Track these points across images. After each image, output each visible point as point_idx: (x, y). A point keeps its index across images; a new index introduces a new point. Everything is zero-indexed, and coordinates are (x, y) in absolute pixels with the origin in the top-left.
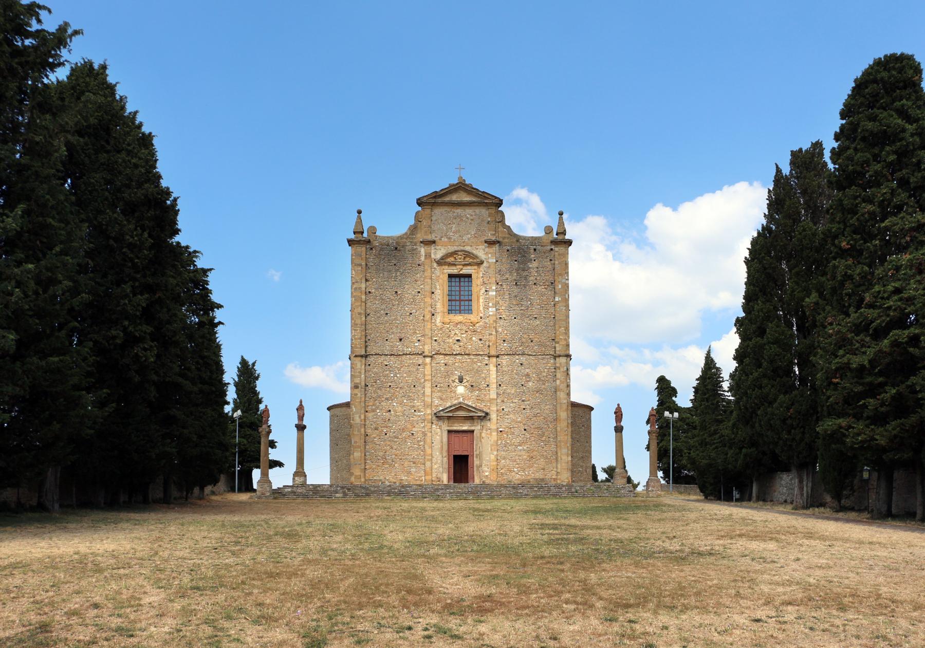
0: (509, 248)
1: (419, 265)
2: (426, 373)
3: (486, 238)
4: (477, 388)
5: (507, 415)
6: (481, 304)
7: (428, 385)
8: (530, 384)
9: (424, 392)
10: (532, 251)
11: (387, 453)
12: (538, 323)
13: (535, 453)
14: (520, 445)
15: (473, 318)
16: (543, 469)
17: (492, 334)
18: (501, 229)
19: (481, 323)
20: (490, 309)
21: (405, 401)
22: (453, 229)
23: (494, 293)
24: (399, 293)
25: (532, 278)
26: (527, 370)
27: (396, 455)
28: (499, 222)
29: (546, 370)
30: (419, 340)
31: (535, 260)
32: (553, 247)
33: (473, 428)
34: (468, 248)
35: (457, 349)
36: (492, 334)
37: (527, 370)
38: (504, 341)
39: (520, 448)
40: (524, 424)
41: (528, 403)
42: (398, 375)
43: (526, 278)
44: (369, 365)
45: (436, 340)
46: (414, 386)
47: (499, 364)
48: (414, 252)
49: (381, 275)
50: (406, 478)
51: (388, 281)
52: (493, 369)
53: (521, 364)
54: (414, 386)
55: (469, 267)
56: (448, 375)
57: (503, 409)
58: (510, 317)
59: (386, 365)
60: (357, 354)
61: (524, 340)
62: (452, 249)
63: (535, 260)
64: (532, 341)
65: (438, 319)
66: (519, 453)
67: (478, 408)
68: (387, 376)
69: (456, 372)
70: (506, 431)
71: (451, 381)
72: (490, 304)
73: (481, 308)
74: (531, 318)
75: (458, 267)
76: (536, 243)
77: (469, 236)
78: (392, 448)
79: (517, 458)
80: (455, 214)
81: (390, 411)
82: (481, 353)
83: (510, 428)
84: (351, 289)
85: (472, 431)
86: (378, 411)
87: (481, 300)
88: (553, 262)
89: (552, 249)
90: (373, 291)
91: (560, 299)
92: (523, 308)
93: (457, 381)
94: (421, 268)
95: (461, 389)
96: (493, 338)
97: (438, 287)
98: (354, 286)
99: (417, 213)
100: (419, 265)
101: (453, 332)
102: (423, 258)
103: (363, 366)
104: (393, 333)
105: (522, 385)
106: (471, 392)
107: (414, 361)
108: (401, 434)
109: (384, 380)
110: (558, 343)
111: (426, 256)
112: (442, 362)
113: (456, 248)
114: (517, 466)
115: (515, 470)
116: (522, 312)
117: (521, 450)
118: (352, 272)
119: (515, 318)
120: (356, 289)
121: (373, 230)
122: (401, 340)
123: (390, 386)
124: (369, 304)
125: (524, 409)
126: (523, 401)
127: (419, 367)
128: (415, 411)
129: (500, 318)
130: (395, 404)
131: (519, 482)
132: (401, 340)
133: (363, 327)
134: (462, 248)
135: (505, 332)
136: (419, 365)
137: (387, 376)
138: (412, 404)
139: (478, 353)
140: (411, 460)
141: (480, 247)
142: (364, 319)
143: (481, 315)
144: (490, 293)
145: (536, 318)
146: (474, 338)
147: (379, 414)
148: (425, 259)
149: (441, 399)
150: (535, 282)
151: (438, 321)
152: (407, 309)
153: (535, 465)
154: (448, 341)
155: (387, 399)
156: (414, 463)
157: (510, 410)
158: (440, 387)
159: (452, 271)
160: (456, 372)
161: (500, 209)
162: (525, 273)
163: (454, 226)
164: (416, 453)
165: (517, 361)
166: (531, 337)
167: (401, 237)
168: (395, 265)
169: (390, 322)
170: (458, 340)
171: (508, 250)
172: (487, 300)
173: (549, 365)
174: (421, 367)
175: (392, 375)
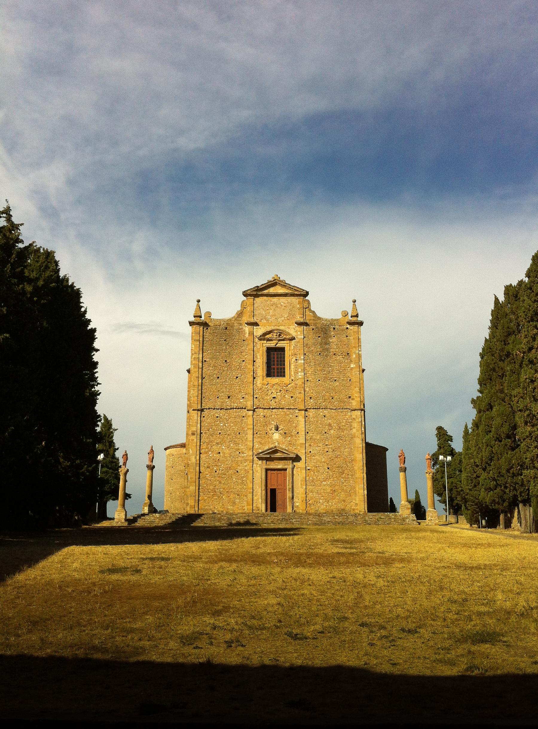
0: (314, 327)
1: (244, 340)
2: (249, 423)
3: (296, 320)
4: (289, 435)
5: (314, 456)
6: (292, 369)
7: (250, 432)
8: (332, 432)
9: (247, 438)
10: (332, 329)
11: (217, 487)
12: (338, 384)
13: (337, 488)
14: (324, 481)
15: (285, 380)
16: (344, 501)
17: (301, 393)
18: (308, 313)
19: (292, 384)
20: (300, 374)
21: (232, 445)
22: (271, 313)
23: (303, 361)
24: (228, 361)
25: (331, 350)
26: (330, 421)
27: (224, 489)
28: (306, 308)
29: (344, 421)
30: (243, 398)
31: (334, 336)
32: (348, 326)
33: (286, 467)
34: (282, 328)
35: (273, 404)
36: (301, 393)
37: (330, 421)
38: (311, 398)
39: (325, 483)
40: (328, 464)
41: (331, 446)
42: (226, 425)
43: (327, 350)
44: (204, 417)
45: (256, 398)
46: (239, 433)
47: (307, 416)
48: (240, 331)
49: (215, 348)
50: (231, 507)
51: (219, 352)
52: (301, 419)
53: (325, 416)
54: (239, 433)
55: (282, 342)
56: (266, 424)
57: (310, 452)
58: (315, 380)
59: (217, 417)
60: (194, 408)
61: (326, 397)
62: (269, 329)
63: (334, 336)
64: (333, 398)
65: (259, 382)
66: (324, 488)
67: (290, 450)
68: (218, 425)
69: (273, 422)
70: (313, 469)
71: (268, 430)
72: (300, 370)
73: (293, 373)
74: (331, 380)
75: (274, 342)
76: (335, 324)
77: (283, 319)
78: (220, 483)
79: (322, 491)
80: (272, 302)
81: (219, 453)
82: (292, 407)
83: (316, 467)
84: (191, 358)
85: (286, 470)
86: (210, 453)
87: (292, 367)
88: (348, 338)
89: (347, 328)
90: (208, 360)
91: (355, 366)
92: (325, 373)
93: (273, 429)
94: (246, 343)
95: (276, 436)
96: (302, 396)
97: (259, 357)
98: (194, 356)
99: (243, 302)
100: (244, 340)
101: (270, 392)
102: (247, 335)
103: (199, 418)
104: (223, 392)
105: (325, 433)
106: (285, 438)
107: (239, 414)
108: (228, 472)
109: (215, 429)
110: (353, 399)
111: (249, 333)
112: (261, 414)
113: (273, 328)
114: (322, 498)
115: (321, 501)
116: (324, 375)
117: (325, 485)
118: (192, 346)
119: (319, 380)
120: (195, 358)
121: (209, 314)
122: (229, 397)
123: (220, 433)
124: (204, 370)
125: (327, 451)
126: (326, 445)
127: (243, 418)
128: (240, 453)
129: (308, 380)
130: (223, 447)
131: (324, 512)
132: (229, 397)
133: (200, 388)
134: (278, 328)
135: (312, 391)
136: (243, 417)
137: (218, 425)
138: (237, 447)
139: (290, 407)
140: (236, 493)
141: (292, 327)
142: (200, 381)
143: (292, 378)
144: (299, 362)
145: (335, 380)
146: (286, 396)
147: (210, 455)
148: (249, 336)
149: (261, 443)
150: (335, 353)
151: (258, 382)
152: (234, 373)
153: (337, 497)
154: (266, 398)
155: (218, 444)
156: (238, 495)
157: (316, 452)
158: (260, 434)
159: (270, 345)
160: (273, 422)
161: (307, 298)
162: (327, 346)
163: (271, 311)
164: (240, 487)
165: (321, 413)
166: (331, 395)
167: (230, 320)
168: (225, 340)
169: (221, 383)
170: (274, 398)
171: (313, 329)
172: (296, 367)
173: (347, 417)
174: (245, 418)
175: (222, 425)
